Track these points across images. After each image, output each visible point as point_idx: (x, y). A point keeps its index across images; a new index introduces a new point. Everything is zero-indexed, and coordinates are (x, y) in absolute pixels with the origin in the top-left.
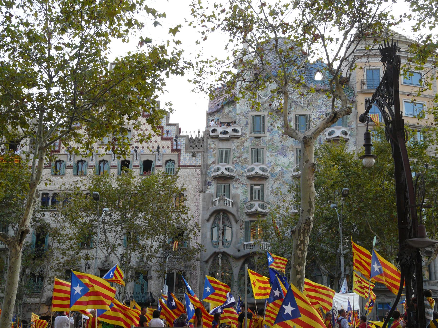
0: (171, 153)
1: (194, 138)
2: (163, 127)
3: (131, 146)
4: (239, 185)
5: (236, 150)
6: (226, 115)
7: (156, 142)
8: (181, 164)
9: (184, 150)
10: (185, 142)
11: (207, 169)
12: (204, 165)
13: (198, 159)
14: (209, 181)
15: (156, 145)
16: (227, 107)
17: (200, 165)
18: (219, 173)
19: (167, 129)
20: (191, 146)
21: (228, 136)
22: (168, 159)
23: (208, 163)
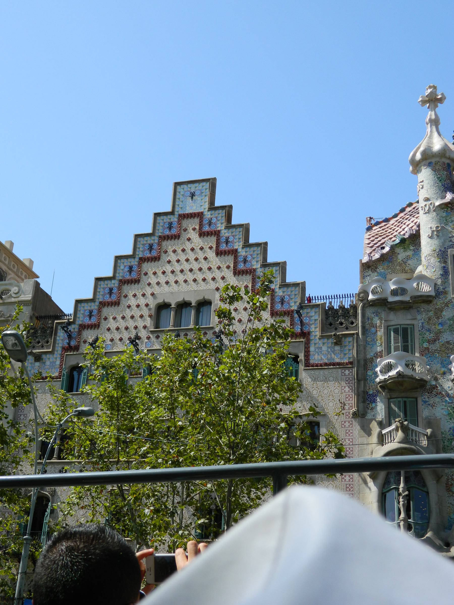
1: (336, 307)
3: (212, 332)
4: (437, 400)
5: (427, 326)
6: (400, 265)
8: (312, 362)
11: (366, 368)
12: (358, 361)
13: (347, 348)
14: (371, 392)
16: (402, 250)
17: (351, 360)
18: (393, 373)
20: (331, 324)
21: (406, 298)
23: (368, 357)
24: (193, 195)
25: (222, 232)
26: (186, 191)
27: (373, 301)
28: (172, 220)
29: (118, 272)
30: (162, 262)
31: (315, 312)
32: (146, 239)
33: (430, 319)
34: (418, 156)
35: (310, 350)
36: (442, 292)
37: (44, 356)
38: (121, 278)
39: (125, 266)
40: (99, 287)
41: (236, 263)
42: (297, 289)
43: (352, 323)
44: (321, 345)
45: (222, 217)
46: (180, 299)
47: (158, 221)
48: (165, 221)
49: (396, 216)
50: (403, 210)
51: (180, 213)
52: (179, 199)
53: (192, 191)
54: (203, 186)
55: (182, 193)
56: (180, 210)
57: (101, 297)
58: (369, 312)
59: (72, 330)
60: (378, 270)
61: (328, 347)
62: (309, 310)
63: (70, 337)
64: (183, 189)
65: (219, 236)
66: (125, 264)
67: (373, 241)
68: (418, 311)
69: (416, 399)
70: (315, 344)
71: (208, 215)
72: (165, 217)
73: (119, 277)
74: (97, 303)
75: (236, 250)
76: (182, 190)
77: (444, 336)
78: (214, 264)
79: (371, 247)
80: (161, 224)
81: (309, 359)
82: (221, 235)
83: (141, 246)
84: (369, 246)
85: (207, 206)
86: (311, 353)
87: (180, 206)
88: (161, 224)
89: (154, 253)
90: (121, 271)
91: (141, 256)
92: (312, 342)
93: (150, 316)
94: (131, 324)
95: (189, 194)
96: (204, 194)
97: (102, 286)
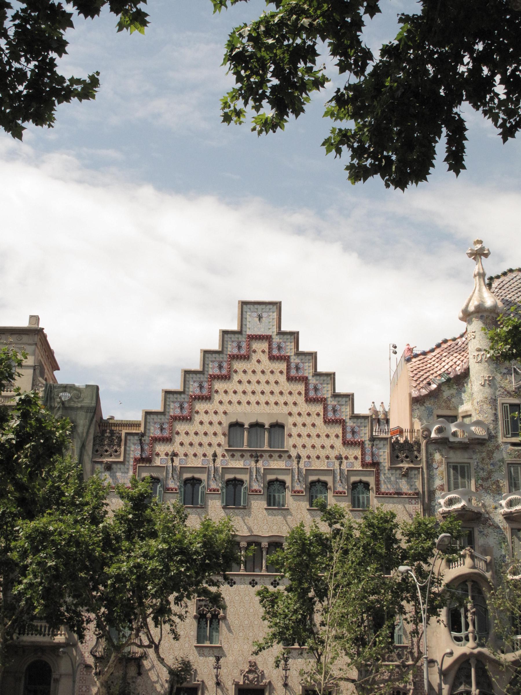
0: (361, 469)
3: (287, 455)
4: (490, 530)
5: (481, 466)
6: (445, 402)
7: (332, 447)
15: (333, 454)
16: (447, 388)
18: (457, 506)
19: (352, 424)
25: (292, 357)
27: (435, 439)
32: (214, 355)
33: (483, 460)
34: (471, 308)
36: (493, 436)
37: (114, 466)
42: (367, 421)
43: (417, 457)
46: (253, 420)
47: (225, 339)
49: (432, 350)
50: (439, 346)
58: (431, 448)
59: (144, 442)
60: (425, 404)
61: (396, 478)
66: (194, 379)
67: (416, 374)
68: (474, 452)
69: (473, 528)
71: (276, 339)
75: (307, 378)
77: (495, 475)
78: (285, 389)
79: (416, 381)
82: (292, 361)
84: (415, 379)
93: (224, 434)
94: (205, 440)
96: (271, 317)
97: (171, 400)
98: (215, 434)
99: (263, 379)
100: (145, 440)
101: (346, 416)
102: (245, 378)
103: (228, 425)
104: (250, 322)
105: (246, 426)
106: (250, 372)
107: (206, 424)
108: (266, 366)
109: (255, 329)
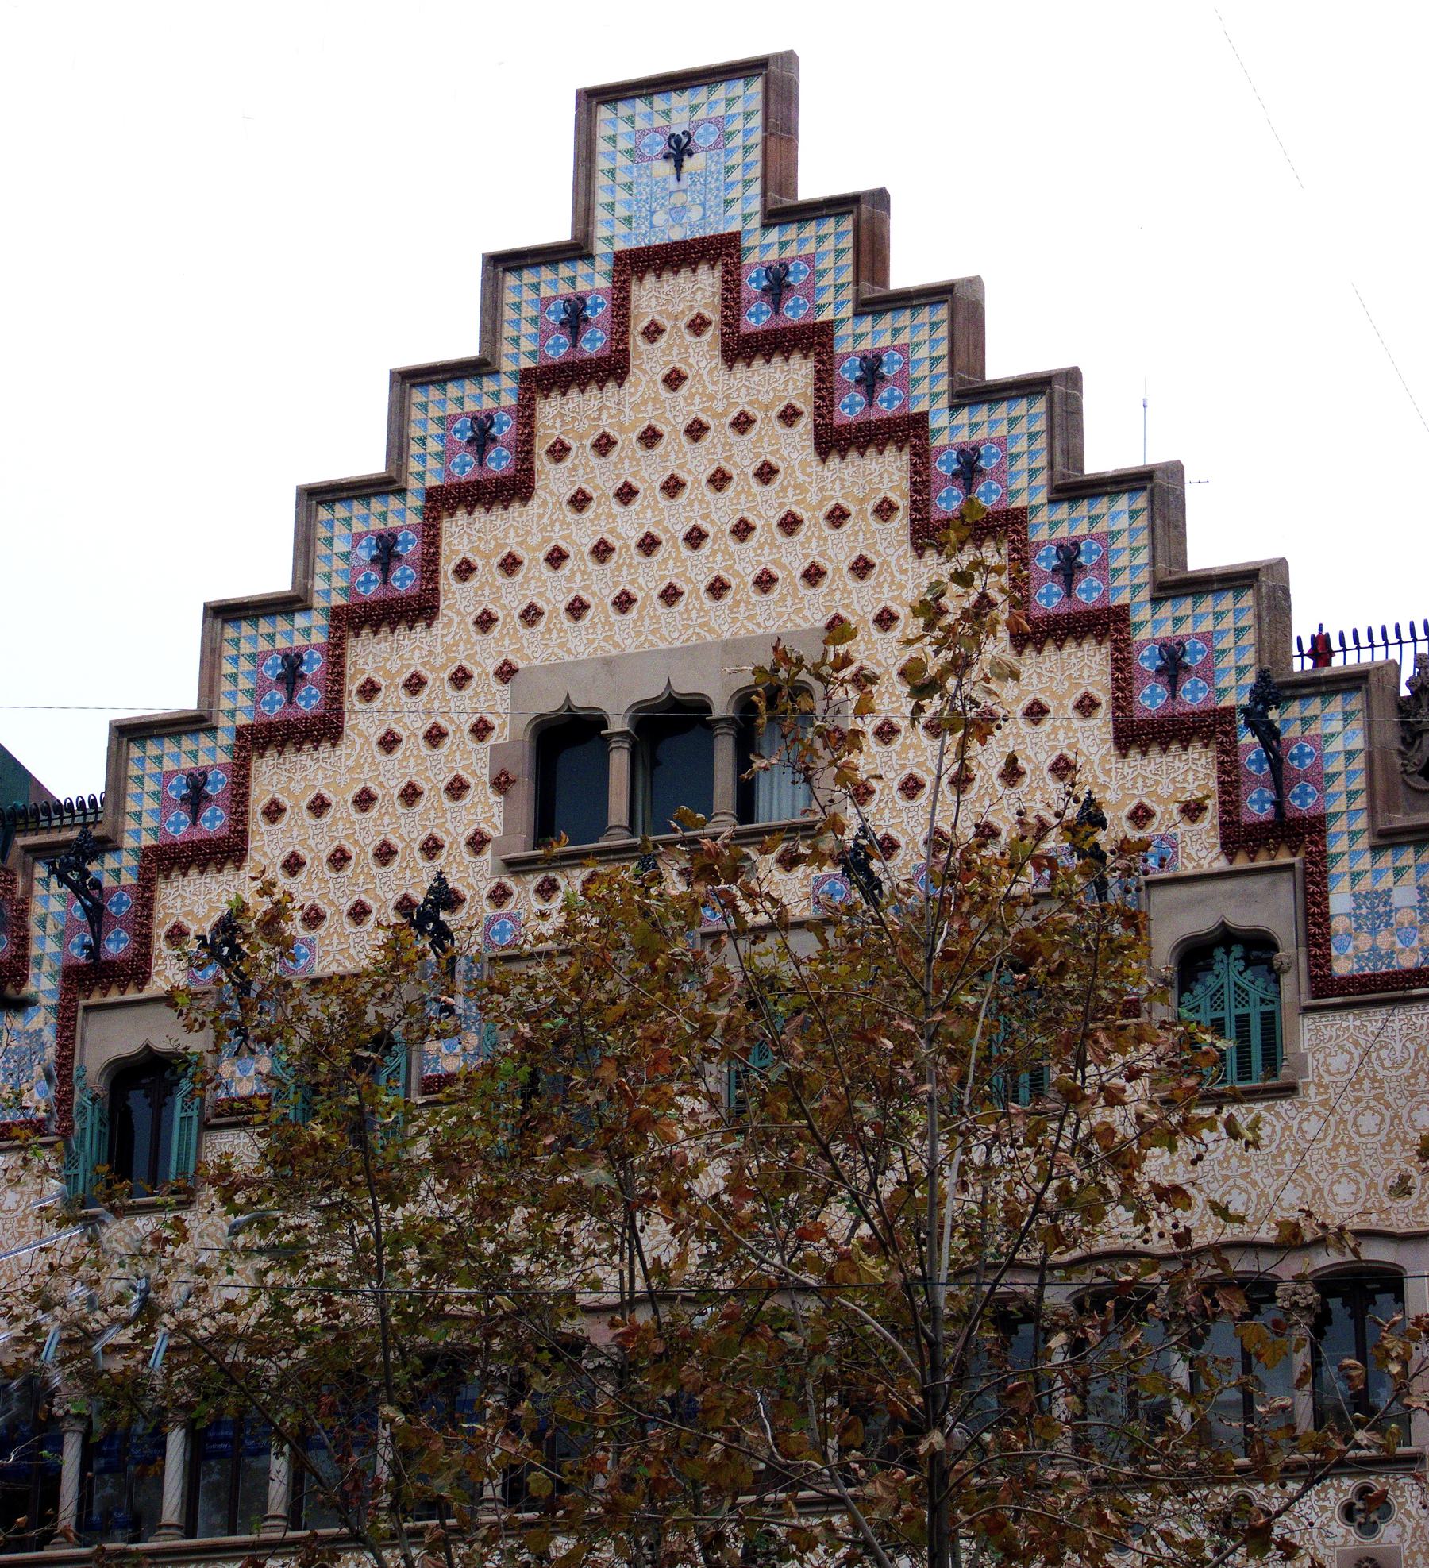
0: (1221, 864)
2: (1121, 615)
8: (1342, 966)
9: (1361, 822)
10: (1358, 742)
19: (1166, 631)
22: (1199, 922)
24: (679, 150)
25: (841, 332)
26: (644, 134)
28: (582, 286)
29: (321, 567)
30: (544, 503)
31: (1347, 716)
32: (453, 390)
35: (1332, 911)
38: (338, 600)
39: (357, 538)
40: (229, 650)
41: (921, 487)
44: (1387, 881)
45: (839, 253)
46: (651, 689)
47: (509, 297)
48: (546, 292)
51: (620, 246)
52: (612, 173)
53: (678, 132)
54: (730, 102)
55: (623, 144)
56: (621, 229)
57: (244, 701)
59: (108, 882)
62: (1314, 706)
63: (96, 915)
64: (631, 120)
65: (830, 353)
66: (358, 527)
70: (1355, 876)
72: (546, 273)
73: (327, 593)
74: (225, 738)
75: (923, 417)
76: (623, 128)
78: (813, 498)
80: (529, 311)
81: (1327, 957)
82: (843, 347)
83: (434, 429)
85: (756, 206)
86: (1338, 925)
87: (621, 211)
88: (529, 311)
89: (499, 459)
90: (339, 564)
91: (433, 481)
92: (1340, 868)
93: (501, 783)
95: (661, 147)
96: (738, 140)
97: (246, 648)
98: (457, 789)
99: (696, 463)
100: (117, 873)
101: (1135, 589)
102: (602, 477)
103: (525, 737)
104: (629, 187)
105: (618, 724)
106: (627, 441)
107: (413, 746)
108: (712, 398)
109: (660, 218)
